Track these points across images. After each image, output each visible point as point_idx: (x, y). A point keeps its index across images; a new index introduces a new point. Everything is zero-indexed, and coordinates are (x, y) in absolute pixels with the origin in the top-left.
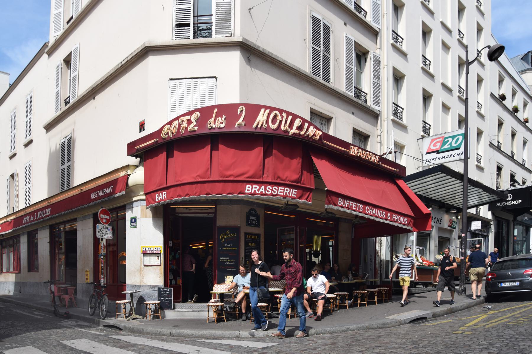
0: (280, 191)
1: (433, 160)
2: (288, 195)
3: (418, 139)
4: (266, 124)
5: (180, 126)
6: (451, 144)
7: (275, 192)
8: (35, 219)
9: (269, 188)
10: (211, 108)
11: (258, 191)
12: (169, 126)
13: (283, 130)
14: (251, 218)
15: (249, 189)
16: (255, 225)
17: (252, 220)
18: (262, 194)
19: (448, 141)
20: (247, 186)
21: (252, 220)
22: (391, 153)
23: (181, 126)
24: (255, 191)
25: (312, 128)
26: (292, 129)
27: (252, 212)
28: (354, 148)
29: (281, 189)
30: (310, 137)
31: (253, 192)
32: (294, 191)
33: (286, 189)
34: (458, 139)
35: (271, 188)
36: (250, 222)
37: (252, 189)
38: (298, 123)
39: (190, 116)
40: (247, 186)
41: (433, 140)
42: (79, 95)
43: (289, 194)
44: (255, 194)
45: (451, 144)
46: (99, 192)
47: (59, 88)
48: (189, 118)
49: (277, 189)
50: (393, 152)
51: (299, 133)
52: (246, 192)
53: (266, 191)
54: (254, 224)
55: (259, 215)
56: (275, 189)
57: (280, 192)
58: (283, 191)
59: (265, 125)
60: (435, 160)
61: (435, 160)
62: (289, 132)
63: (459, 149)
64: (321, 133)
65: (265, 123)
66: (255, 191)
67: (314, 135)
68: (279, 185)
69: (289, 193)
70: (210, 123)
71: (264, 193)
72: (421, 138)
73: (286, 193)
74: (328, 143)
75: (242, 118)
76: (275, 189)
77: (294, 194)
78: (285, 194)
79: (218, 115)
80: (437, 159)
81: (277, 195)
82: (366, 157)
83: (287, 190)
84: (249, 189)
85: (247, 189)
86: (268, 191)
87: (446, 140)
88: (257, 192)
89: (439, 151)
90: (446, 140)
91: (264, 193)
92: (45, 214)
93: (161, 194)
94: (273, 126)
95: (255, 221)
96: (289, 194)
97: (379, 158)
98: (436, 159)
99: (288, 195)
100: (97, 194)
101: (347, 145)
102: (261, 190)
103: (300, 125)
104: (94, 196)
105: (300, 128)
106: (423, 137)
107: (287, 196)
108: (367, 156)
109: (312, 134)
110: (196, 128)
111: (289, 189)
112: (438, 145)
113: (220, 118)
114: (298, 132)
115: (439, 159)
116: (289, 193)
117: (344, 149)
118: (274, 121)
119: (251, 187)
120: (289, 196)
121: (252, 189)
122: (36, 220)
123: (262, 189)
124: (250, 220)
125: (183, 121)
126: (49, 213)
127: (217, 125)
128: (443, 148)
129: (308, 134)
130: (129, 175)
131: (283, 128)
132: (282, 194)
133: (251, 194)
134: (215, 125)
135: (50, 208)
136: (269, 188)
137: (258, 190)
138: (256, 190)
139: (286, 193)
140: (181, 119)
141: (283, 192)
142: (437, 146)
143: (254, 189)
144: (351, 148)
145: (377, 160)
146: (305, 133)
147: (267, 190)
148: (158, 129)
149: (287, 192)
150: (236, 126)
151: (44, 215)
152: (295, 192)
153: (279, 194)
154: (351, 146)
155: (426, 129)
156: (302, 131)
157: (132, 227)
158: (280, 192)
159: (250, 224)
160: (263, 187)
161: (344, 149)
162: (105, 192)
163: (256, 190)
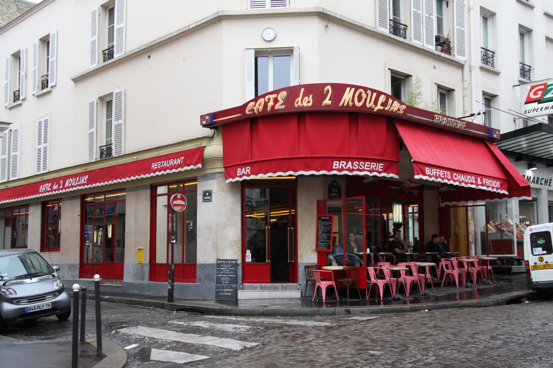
0: (366, 166)
1: (533, 111)
2: (375, 169)
3: (514, 86)
4: (352, 102)
5: (266, 104)
7: (361, 167)
8: (61, 187)
9: (356, 164)
10: (299, 87)
11: (346, 167)
12: (254, 103)
13: (368, 107)
14: (333, 190)
16: (337, 197)
17: (334, 192)
18: (349, 170)
20: (335, 162)
21: (334, 192)
22: (479, 114)
23: (268, 105)
24: (342, 167)
27: (333, 184)
28: (439, 116)
29: (367, 164)
30: (394, 111)
31: (340, 168)
33: (372, 163)
35: (358, 163)
37: (339, 165)
38: (382, 98)
39: (276, 95)
40: (335, 162)
41: (533, 88)
42: (127, 51)
46: (164, 163)
48: (276, 97)
49: (364, 164)
50: (482, 113)
51: (384, 109)
52: (334, 168)
53: (353, 167)
54: (335, 197)
55: (341, 187)
57: (367, 167)
58: (369, 166)
60: (537, 111)
61: (537, 111)
62: (374, 109)
64: (405, 107)
66: (342, 167)
67: (399, 110)
68: (365, 160)
69: (376, 167)
70: (298, 101)
71: (351, 168)
72: (518, 84)
73: (373, 168)
74: (412, 115)
77: (381, 169)
78: (371, 169)
79: (306, 94)
80: (539, 109)
82: (452, 125)
83: (373, 165)
84: (336, 165)
85: (334, 165)
86: (355, 167)
87: (549, 88)
88: (344, 168)
89: (542, 101)
90: (549, 88)
91: (351, 168)
92: (78, 182)
93: (244, 169)
94: (359, 104)
95: (337, 193)
97: (465, 124)
98: (537, 110)
100: (161, 164)
101: (431, 115)
102: (348, 166)
103: (384, 101)
104: (156, 167)
105: (384, 104)
106: (522, 83)
108: (453, 124)
109: (396, 109)
110: (283, 107)
112: (540, 93)
113: (307, 98)
114: (382, 108)
115: (541, 110)
116: (376, 167)
117: (427, 119)
119: (338, 163)
121: (339, 165)
122: (62, 189)
123: (349, 165)
124: (332, 192)
125: (269, 99)
126: (85, 181)
127: (305, 104)
128: (546, 97)
129: (392, 109)
130: (205, 147)
132: (369, 169)
133: (339, 170)
134: (302, 104)
135: (87, 176)
136: (356, 164)
137: (346, 166)
139: (373, 168)
140: (267, 97)
141: (370, 167)
142: (538, 94)
143: (341, 165)
144: (436, 117)
145: (464, 126)
147: (354, 166)
149: (374, 167)
151: (77, 184)
152: (381, 166)
153: (365, 168)
154: (436, 116)
155: (525, 71)
156: (386, 107)
158: (367, 167)
159: (332, 197)
160: (350, 163)
161: (427, 119)
162: (172, 162)
163: (343, 165)
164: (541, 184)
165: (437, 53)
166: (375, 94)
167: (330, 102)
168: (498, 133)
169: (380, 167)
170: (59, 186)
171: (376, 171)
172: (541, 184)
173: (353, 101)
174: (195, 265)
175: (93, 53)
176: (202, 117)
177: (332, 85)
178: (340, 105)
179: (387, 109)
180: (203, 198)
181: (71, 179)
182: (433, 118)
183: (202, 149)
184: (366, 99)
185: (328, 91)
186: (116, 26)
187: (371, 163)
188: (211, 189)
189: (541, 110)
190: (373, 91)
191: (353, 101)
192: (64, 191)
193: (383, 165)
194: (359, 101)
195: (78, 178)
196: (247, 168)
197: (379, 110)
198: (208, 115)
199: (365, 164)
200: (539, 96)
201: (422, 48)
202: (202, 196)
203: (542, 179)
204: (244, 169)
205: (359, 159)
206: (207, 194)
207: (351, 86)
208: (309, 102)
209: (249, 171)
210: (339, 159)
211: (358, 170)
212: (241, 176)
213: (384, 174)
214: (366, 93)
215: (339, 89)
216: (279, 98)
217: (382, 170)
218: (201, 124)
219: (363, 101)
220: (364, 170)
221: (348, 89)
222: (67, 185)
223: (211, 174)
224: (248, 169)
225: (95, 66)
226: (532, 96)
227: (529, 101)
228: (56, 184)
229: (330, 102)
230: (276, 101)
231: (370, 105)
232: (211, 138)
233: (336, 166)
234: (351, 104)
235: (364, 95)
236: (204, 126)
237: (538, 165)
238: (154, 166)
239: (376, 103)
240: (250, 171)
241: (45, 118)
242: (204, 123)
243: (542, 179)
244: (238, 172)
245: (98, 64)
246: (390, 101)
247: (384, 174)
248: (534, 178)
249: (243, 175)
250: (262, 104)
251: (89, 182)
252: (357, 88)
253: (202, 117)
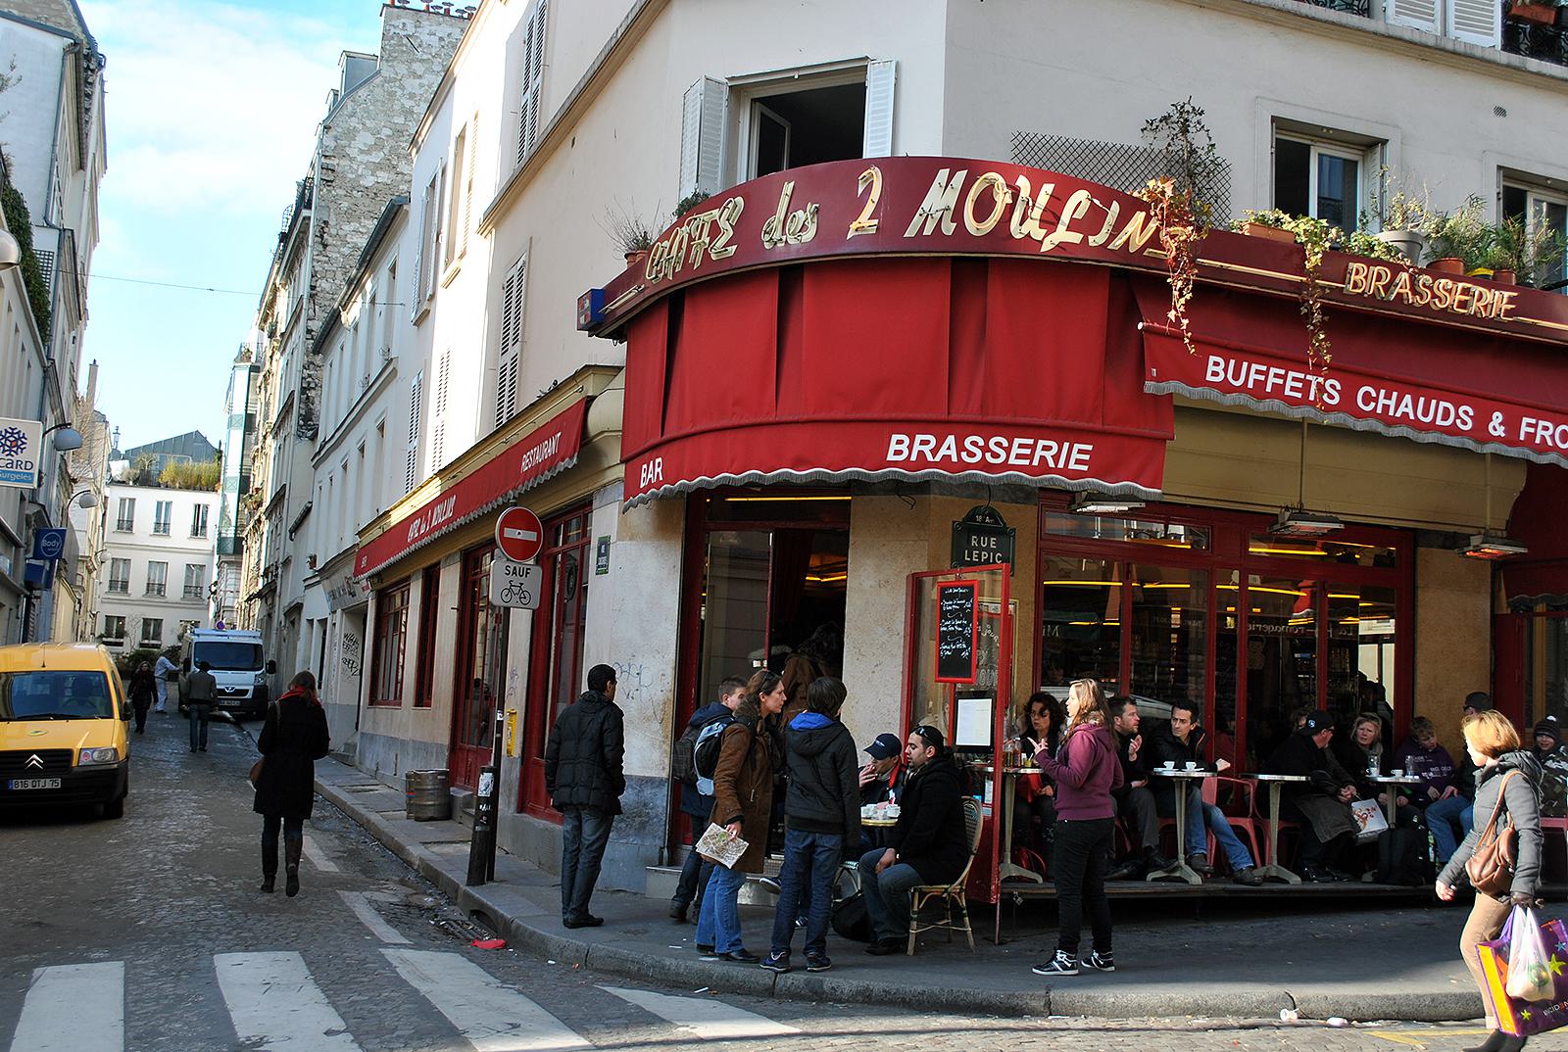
0: (1015, 450)
2: (1051, 464)
7: (996, 455)
9: (974, 443)
15: (899, 447)
20: (895, 437)
21: (980, 549)
24: (921, 453)
29: (1021, 446)
31: (913, 458)
32: (1075, 450)
33: (1041, 443)
35: (981, 443)
36: (971, 556)
37: (910, 447)
40: (895, 437)
43: (1056, 464)
51: (1085, 240)
52: (891, 457)
53: (964, 455)
56: (999, 444)
57: (1018, 457)
58: (1028, 451)
59: (948, 228)
62: (1041, 242)
65: (948, 215)
66: (921, 453)
67: (1155, 241)
68: (1011, 430)
69: (1056, 458)
71: (954, 459)
73: (1043, 458)
75: (870, 208)
76: (999, 444)
77: (1078, 462)
78: (1035, 463)
81: (1005, 466)
83: (1046, 448)
84: (899, 447)
85: (893, 447)
86: (971, 455)
88: (930, 458)
91: (954, 459)
96: (1056, 464)
99: (1051, 464)
102: (943, 451)
105: (1090, 223)
107: (1050, 471)
111: (1054, 444)
114: (1076, 238)
116: (1056, 458)
119: (907, 441)
120: (1056, 471)
121: (910, 447)
123: (949, 448)
131: (1016, 230)
132: (1027, 462)
136: (974, 443)
137: (934, 452)
138: (926, 449)
139: (1043, 458)
141: (1031, 457)
143: (917, 447)
146: (1112, 237)
147: (966, 450)
153: (1012, 461)
158: (1018, 457)
160: (951, 440)
163: (926, 449)
171: (1056, 471)
173: (958, 215)
179: (1095, 241)
184: (1010, 209)
187: (1036, 443)
191: (958, 215)
193: (1089, 447)
197: (1062, 246)
199: (1011, 444)
205: (986, 428)
207: (954, 165)
209: (658, 470)
216: (723, 224)
217: (1085, 468)
221: (944, 174)
229: (876, 222)
231: (1025, 229)
233: (898, 453)
234: (948, 228)
235: (1002, 198)
239: (1050, 221)
240: (662, 471)
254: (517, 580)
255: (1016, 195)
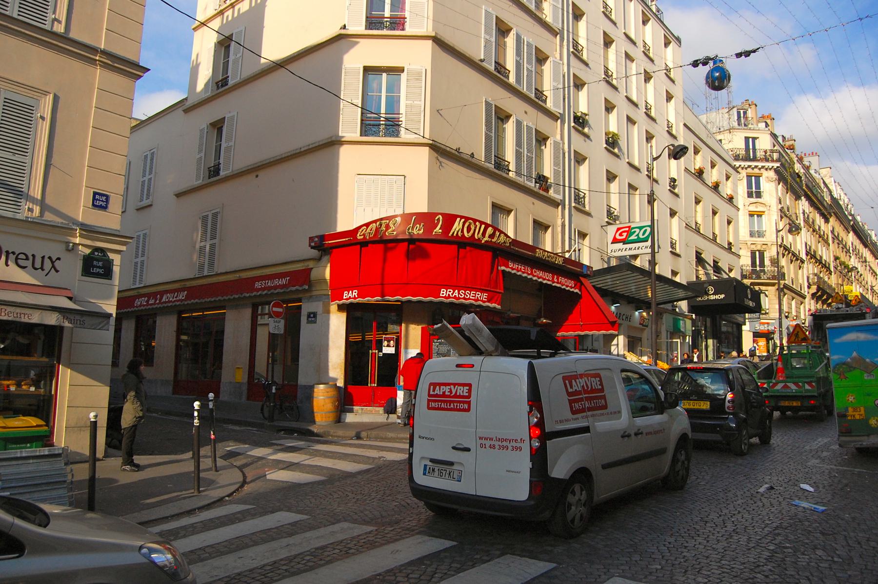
0: (472, 295)
6: (638, 235)
7: (467, 296)
8: (158, 302)
12: (365, 227)
15: (443, 292)
18: (455, 297)
19: (635, 232)
20: (442, 290)
24: (449, 294)
25: (502, 235)
26: (484, 237)
34: (646, 230)
37: (446, 293)
38: (490, 230)
40: (442, 290)
41: (618, 229)
44: (449, 297)
45: (638, 235)
47: (203, 155)
52: (441, 295)
57: (472, 296)
63: (647, 241)
66: (449, 294)
67: (504, 242)
69: (480, 297)
75: (439, 226)
77: (485, 298)
80: (624, 250)
81: (469, 299)
83: (478, 294)
85: (442, 292)
86: (461, 295)
92: (176, 297)
93: (351, 292)
100: (265, 284)
102: (454, 294)
105: (492, 236)
112: (625, 234)
115: (625, 250)
116: (480, 297)
118: (469, 229)
121: (446, 293)
122: (158, 304)
125: (381, 225)
126: (183, 297)
128: (629, 239)
133: (445, 297)
135: (186, 292)
137: (452, 294)
138: (450, 293)
140: (378, 223)
141: (475, 297)
143: (448, 293)
148: (352, 229)
150: (434, 233)
154: (538, 250)
157: (308, 322)
158: (472, 296)
160: (457, 291)
164: (623, 320)
165: (536, 189)
166: (483, 226)
167: (440, 231)
168: (591, 270)
169: (484, 297)
170: (156, 301)
171: (480, 300)
172: (623, 320)
174: (297, 385)
175: (198, 169)
176: (311, 239)
177: (442, 214)
178: (450, 235)
180: (307, 320)
181: (168, 294)
182: (535, 252)
183: (308, 271)
185: (439, 219)
186: (224, 145)
188: (315, 311)
189: (625, 250)
190: (482, 223)
192: (160, 305)
194: (468, 231)
195: (176, 294)
196: (354, 291)
197: (486, 242)
198: (317, 237)
200: (624, 237)
201: (523, 184)
202: (306, 318)
203: (624, 315)
204: (351, 292)
206: (312, 316)
207: (462, 217)
208: (419, 230)
209: (356, 294)
210: (447, 287)
211: (464, 298)
212: (347, 299)
213: (488, 304)
214: (475, 224)
215: (450, 219)
216: (391, 225)
218: (310, 245)
219: (472, 232)
220: (469, 299)
221: (458, 219)
222: (164, 300)
223: (316, 296)
224: (355, 293)
225: (200, 182)
226: (618, 237)
227: (615, 241)
228: (153, 299)
229: (440, 231)
230: (388, 227)
232: (319, 259)
233: (443, 294)
235: (473, 228)
236: (312, 248)
237: (621, 302)
238: (258, 285)
239: (484, 234)
241: (144, 232)
242: (313, 244)
243: (624, 315)
244: (345, 295)
245: (203, 181)
246: (497, 233)
247: (488, 304)
248: (617, 313)
249: (350, 298)
250: (374, 229)
251: (188, 297)
252: (467, 219)
253: (311, 239)
254: (277, 324)
255: (476, 227)
